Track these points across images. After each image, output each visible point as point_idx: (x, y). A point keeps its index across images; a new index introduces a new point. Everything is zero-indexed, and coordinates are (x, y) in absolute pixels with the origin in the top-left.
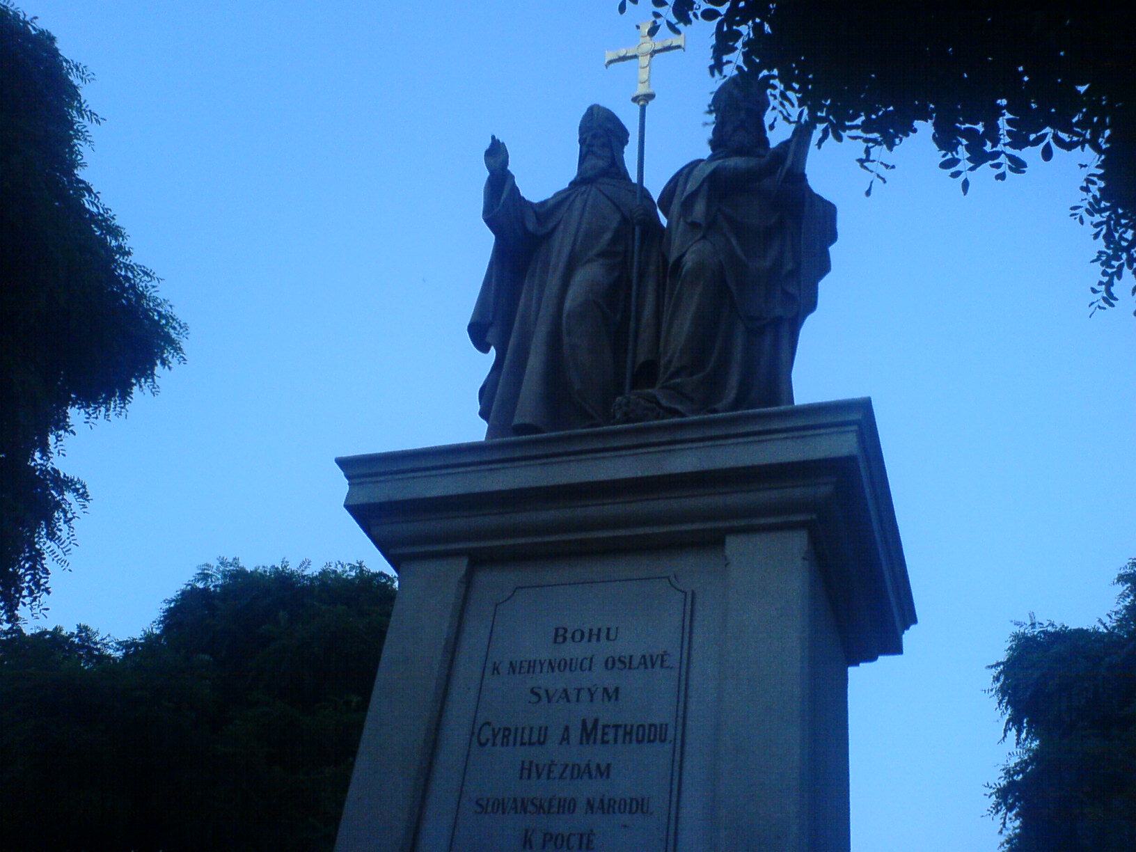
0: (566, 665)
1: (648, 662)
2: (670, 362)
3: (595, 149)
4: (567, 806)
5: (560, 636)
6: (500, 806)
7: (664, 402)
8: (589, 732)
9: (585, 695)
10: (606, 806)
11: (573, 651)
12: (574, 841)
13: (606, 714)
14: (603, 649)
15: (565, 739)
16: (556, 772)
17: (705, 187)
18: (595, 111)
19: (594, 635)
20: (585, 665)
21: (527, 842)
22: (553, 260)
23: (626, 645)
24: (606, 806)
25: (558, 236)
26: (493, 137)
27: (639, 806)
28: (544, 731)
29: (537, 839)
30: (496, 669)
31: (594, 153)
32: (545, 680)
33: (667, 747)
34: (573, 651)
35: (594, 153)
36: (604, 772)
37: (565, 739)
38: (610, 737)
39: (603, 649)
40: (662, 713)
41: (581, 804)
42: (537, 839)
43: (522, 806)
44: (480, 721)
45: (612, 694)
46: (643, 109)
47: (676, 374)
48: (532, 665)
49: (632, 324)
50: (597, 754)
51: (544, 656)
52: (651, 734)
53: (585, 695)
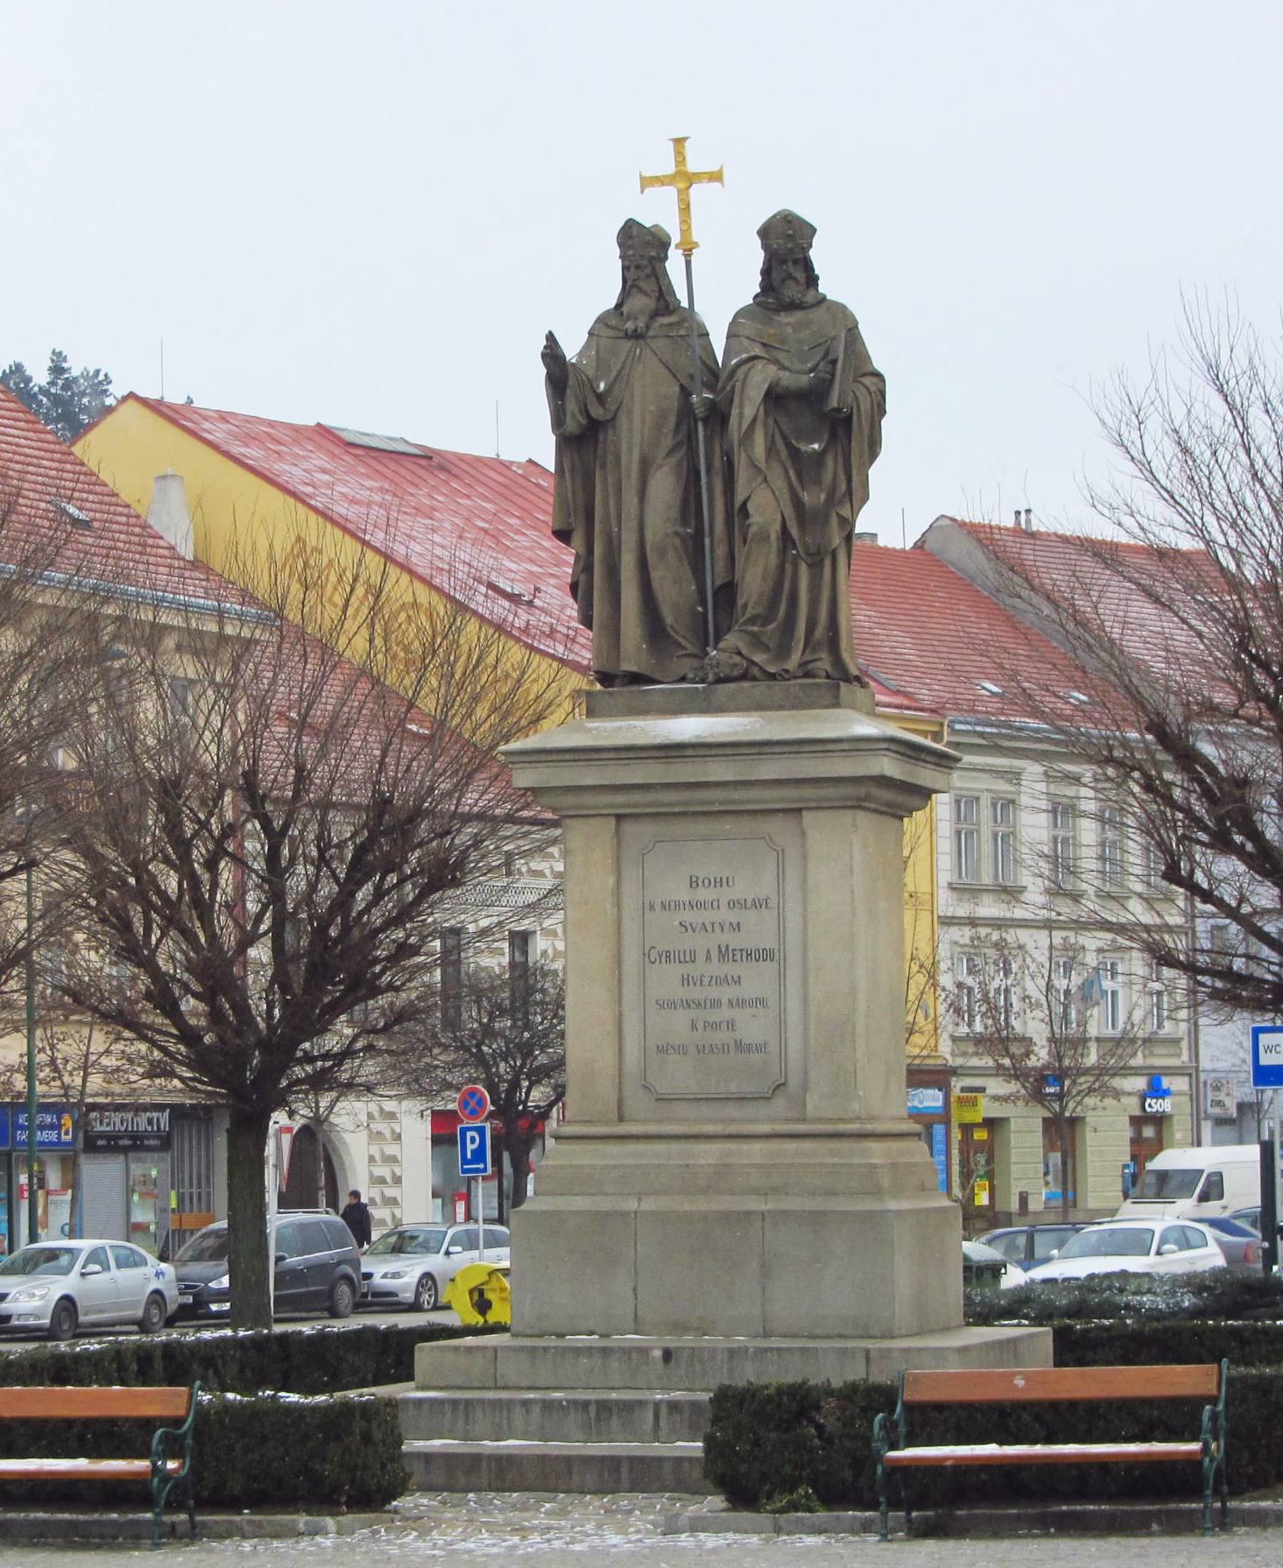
0: (700, 905)
1: (758, 904)
2: (745, 606)
3: (641, 283)
4: (716, 1004)
5: (694, 883)
6: (672, 1005)
7: (744, 651)
8: (725, 954)
9: (717, 928)
10: (741, 1003)
11: (703, 894)
12: (724, 1026)
13: (734, 941)
14: (726, 894)
15: (708, 958)
16: (706, 981)
18: (635, 231)
19: (719, 882)
20: (714, 905)
21: (694, 1027)
23: (740, 891)
24: (741, 1003)
25: (623, 421)
26: (551, 337)
27: (761, 1002)
28: (693, 954)
29: (700, 1025)
30: (652, 907)
31: (640, 290)
32: (689, 916)
33: (775, 964)
34: (703, 894)
35: (640, 290)
36: (738, 981)
37: (708, 958)
38: (738, 957)
39: (726, 894)
40: (769, 942)
41: (725, 1001)
42: (700, 1025)
43: (687, 1004)
44: (647, 946)
45: (737, 927)
46: (688, 264)
47: (752, 620)
48: (677, 905)
49: (707, 541)
50: (731, 969)
51: (686, 899)
52: (766, 955)
53: (717, 928)
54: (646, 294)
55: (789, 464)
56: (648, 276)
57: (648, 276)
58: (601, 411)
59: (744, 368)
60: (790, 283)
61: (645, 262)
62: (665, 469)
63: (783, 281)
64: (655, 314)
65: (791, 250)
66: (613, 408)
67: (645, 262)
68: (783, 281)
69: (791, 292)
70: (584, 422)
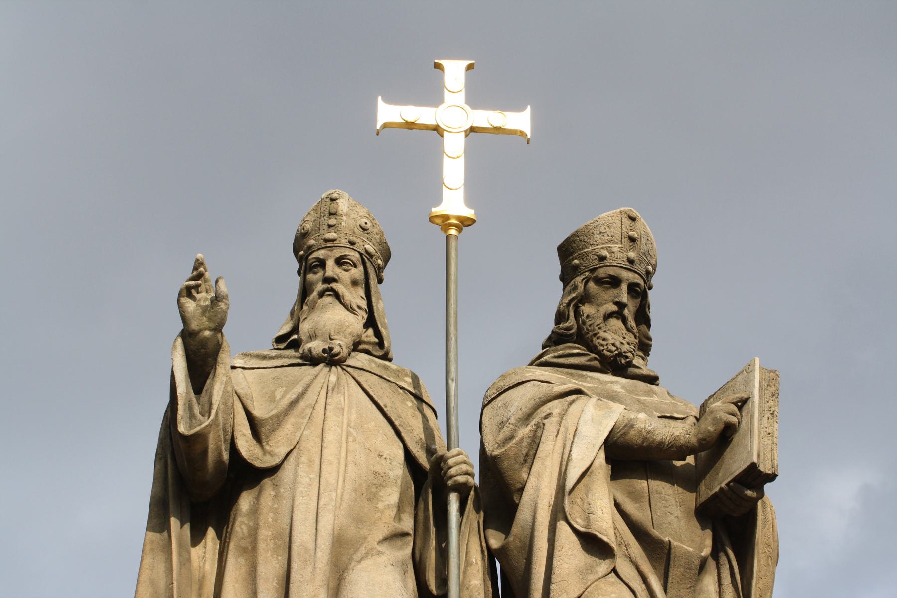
17: (602, 455)
22: (302, 535)
31: (337, 296)
35: (337, 296)
54: (349, 309)
55: (646, 567)
56: (355, 283)
57: (355, 283)
58: (257, 450)
59: (556, 407)
60: (616, 323)
61: (355, 256)
62: (383, 559)
63: (608, 317)
64: (356, 346)
65: (631, 261)
66: (282, 451)
67: (355, 256)
68: (608, 317)
69: (615, 337)
70: (226, 456)
